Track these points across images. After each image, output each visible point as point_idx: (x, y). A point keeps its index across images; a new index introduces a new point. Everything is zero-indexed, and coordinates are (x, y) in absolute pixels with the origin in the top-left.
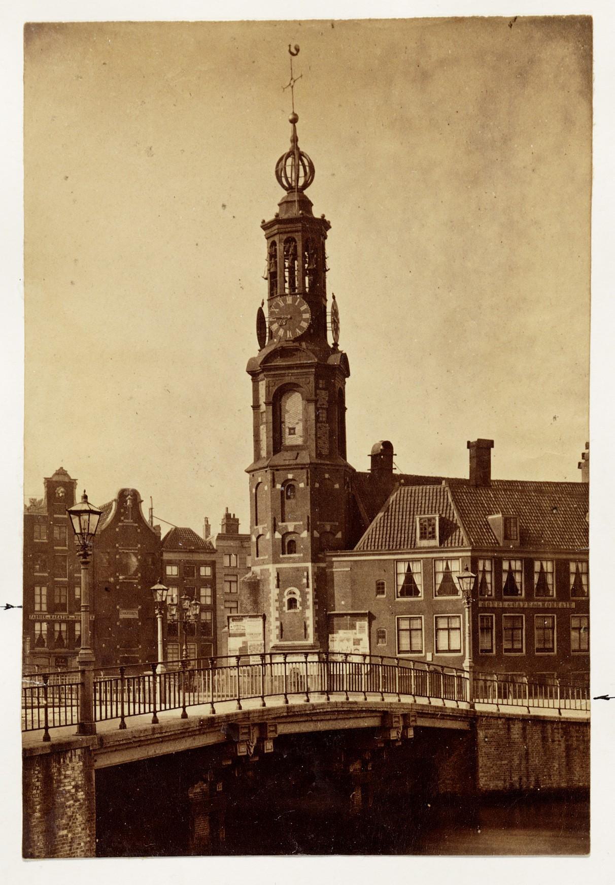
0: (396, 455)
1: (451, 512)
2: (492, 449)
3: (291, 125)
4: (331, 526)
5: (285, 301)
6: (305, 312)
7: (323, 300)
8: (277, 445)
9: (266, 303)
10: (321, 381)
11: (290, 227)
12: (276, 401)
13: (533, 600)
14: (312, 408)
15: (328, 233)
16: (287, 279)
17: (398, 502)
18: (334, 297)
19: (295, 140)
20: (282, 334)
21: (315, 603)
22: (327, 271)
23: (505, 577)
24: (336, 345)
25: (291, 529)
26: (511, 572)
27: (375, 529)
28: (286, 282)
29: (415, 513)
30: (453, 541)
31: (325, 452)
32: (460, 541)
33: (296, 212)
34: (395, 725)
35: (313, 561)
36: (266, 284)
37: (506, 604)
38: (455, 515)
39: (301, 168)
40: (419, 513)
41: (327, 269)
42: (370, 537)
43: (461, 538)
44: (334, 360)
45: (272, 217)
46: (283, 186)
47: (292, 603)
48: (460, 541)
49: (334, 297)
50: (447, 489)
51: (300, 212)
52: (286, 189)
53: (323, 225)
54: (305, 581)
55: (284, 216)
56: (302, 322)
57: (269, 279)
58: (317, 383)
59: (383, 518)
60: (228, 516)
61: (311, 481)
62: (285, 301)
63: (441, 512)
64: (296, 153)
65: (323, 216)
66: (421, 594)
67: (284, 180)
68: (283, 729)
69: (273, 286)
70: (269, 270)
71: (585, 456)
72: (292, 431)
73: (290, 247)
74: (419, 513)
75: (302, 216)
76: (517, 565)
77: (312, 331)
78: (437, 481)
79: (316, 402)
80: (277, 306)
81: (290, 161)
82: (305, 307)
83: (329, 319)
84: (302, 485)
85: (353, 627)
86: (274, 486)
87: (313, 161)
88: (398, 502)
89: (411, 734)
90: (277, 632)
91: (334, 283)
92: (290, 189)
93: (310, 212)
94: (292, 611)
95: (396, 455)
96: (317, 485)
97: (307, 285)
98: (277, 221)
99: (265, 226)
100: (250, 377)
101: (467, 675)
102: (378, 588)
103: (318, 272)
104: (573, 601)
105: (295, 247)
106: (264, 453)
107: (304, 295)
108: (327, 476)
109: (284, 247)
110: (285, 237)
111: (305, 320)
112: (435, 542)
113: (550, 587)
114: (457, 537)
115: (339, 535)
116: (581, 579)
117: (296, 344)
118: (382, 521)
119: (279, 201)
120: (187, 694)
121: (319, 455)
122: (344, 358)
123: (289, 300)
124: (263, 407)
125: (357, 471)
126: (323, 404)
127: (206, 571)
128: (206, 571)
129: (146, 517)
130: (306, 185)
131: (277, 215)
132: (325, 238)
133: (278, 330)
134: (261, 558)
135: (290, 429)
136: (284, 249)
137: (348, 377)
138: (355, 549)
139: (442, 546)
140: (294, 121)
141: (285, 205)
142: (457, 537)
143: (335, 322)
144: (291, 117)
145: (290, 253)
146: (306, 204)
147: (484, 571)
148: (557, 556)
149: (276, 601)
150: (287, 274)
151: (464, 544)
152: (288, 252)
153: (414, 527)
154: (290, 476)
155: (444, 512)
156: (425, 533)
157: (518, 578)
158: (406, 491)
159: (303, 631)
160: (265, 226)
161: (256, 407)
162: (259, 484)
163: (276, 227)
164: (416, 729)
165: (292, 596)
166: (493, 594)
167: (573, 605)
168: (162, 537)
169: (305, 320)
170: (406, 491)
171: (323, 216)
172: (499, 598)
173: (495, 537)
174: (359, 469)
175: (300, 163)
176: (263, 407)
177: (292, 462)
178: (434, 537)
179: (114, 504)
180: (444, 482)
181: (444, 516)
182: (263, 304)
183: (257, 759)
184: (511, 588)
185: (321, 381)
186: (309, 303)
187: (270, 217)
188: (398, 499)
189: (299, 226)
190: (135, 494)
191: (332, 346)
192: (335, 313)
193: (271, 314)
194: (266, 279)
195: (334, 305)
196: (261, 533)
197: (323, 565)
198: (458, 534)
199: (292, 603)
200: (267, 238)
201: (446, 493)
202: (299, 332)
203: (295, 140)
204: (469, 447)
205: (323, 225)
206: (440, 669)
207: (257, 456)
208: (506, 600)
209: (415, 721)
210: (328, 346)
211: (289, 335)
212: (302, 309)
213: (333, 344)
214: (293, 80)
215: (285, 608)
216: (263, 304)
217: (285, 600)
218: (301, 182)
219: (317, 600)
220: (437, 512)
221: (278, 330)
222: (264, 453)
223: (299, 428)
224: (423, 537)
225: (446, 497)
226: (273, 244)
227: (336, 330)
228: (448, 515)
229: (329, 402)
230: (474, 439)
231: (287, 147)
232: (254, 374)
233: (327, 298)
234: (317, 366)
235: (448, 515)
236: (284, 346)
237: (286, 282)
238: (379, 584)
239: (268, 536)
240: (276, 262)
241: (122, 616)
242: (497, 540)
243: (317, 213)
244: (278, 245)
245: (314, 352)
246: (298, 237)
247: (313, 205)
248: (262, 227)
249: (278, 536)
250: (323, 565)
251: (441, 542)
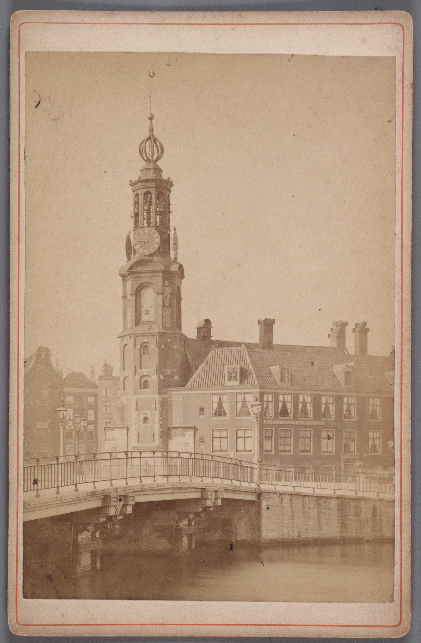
0: (213, 328)
1: (248, 364)
2: (274, 325)
3: (149, 121)
4: (171, 372)
5: (144, 231)
6: (156, 238)
7: (168, 230)
8: (138, 321)
9: (132, 232)
10: (166, 281)
11: (148, 184)
12: (137, 294)
13: (298, 420)
14: (160, 297)
15: (172, 189)
16: (145, 217)
17: (214, 358)
18: (175, 229)
19: (152, 130)
20: (141, 252)
21: (160, 420)
22: (171, 212)
23: (281, 405)
24: (176, 258)
25: (145, 374)
26: (284, 403)
27: (199, 375)
28: (144, 219)
29: (225, 365)
30: (248, 382)
31: (168, 325)
32: (253, 382)
33: (151, 175)
34: (209, 497)
35: (159, 394)
36: (132, 221)
37: (281, 422)
38: (250, 366)
39: (155, 148)
40: (227, 364)
41: (171, 211)
42: (196, 379)
43: (253, 380)
44: (174, 268)
45: (137, 179)
47: (145, 419)
48: (253, 382)
49: (175, 229)
50: (245, 349)
51: (155, 175)
52: (146, 161)
53: (168, 184)
54: (154, 406)
55: (143, 178)
56: (155, 244)
57: (134, 217)
58: (163, 282)
59: (204, 367)
60: (106, 365)
61: (159, 344)
62: (144, 231)
63: (241, 364)
64: (152, 139)
65: (169, 179)
66: (228, 415)
67: (144, 155)
68: (140, 499)
69: (136, 221)
70: (134, 212)
71: (333, 330)
72: (147, 312)
73: (147, 197)
74: (227, 364)
75: (155, 178)
76: (289, 398)
77: (161, 250)
78: (239, 344)
79: (163, 294)
80: (139, 234)
81: (148, 143)
82: (157, 235)
83: (172, 242)
84: (153, 346)
85: (184, 435)
86: (135, 346)
87: (163, 144)
88: (214, 358)
89: (219, 503)
90: (136, 437)
91: (174, 220)
92: (148, 160)
93: (161, 175)
94: (146, 425)
95: (213, 328)
96: (163, 346)
97: (158, 221)
98: (140, 181)
99: (132, 184)
100: (121, 278)
101: (255, 466)
102: (201, 411)
103: (165, 212)
104: (323, 421)
105: (151, 197)
106: (129, 326)
107: (156, 227)
108: (169, 340)
109: (144, 197)
110: (144, 191)
111: (156, 243)
112: (237, 383)
113: (309, 412)
114: (251, 380)
115: (176, 378)
116: (328, 408)
117: (151, 258)
118: (204, 369)
119: (141, 169)
120: (78, 476)
121: (164, 327)
122: (181, 267)
123: (147, 230)
124: (129, 297)
125: (189, 337)
126: (167, 296)
127: (91, 400)
128: (91, 400)
129: (54, 365)
130: (158, 158)
131: (140, 178)
132: (170, 192)
133: (139, 249)
134: (126, 391)
135: (146, 311)
136: (144, 198)
137: (183, 279)
138: (186, 386)
139: (242, 385)
140: (151, 118)
141: (145, 171)
142: (251, 380)
143: (176, 244)
144: (149, 116)
145: (148, 201)
146: (158, 170)
147: (268, 401)
148: (313, 393)
149: (136, 418)
150: (145, 214)
151: (255, 385)
152: (146, 200)
153: (224, 374)
154: (146, 340)
155: (243, 364)
156: (231, 377)
157: (289, 406)
158: (219, 351)
159: (152, 437)
160: (132, 184)
161: (125, 297)
162: (126, 345)
163: (139, 184)
164: (223, 500)
165: (146, 416)
166: (273, 415)
167: (323, 423)
168: (64, 378)
169: (156, 243)
170: (219, 351)
171: (169, 179)
172: (276, 418)
173: (275, 380)
174: (189, 336)
175: (155, 145)
176: (129, 297)
177: (147, 332)
178: (236, 380)
179: (34, 357)
180: (243, 345)
181: (242, 366)
183: (121, 517)
184: (284, 413)
185: (166, 281)
186: (158, 232)
187: (135, 178)
188: (214, 356)
189: (153, 184)
190: (47, 350)
191: (173, 259)
192: (176, 239)
193: (135, 239)
194: (132, 217)
195: (175, 234)
196: (126, 376)
197: (165, 396)
198: (251, 378)
199: (145, 419)
200: (133, 192)
201: (244, 352)
202: (153, 251)
203: (152, 130)
204: (259, 323)
205: (168, 184)
206: (238, 462)
207: (125, 328)
208: (281, 420)
209: (222, 495)
210: (171, 259)
211: (147, 252)
212: (155, 236)
213: (174, 258)
214: (151, 93)
215: (141, 423)
217: (141, 418)
218: (155, 156)
219: (161, 418)
220: (239, 364)
221: (139, 249)
222: (129, 326)
223: (152, 310)
224: (229, 379)
225: (244, 355)
226: (137, 195)
227: (176, 249)
228: (245, 366)
229: (171, 294)
230: (262, 319)
231: (147, 135)
232: (123, 276)
233: (171, 229)
234: (164, 272)
235: (245, 366)
236: (143, 259)
237: (144, 219)
238: (201, 409)
239: (131, 377)
240: (138, 206)
241: (38, 426)
242: (276, 382)
243: (165, 176)
244: (140, 195)
245: (161, 262)
246: (153, 191)
247: (162, 171)
248: (130, 184)
249: (137, 377)
250: (165, 396)
251: (241, 382)
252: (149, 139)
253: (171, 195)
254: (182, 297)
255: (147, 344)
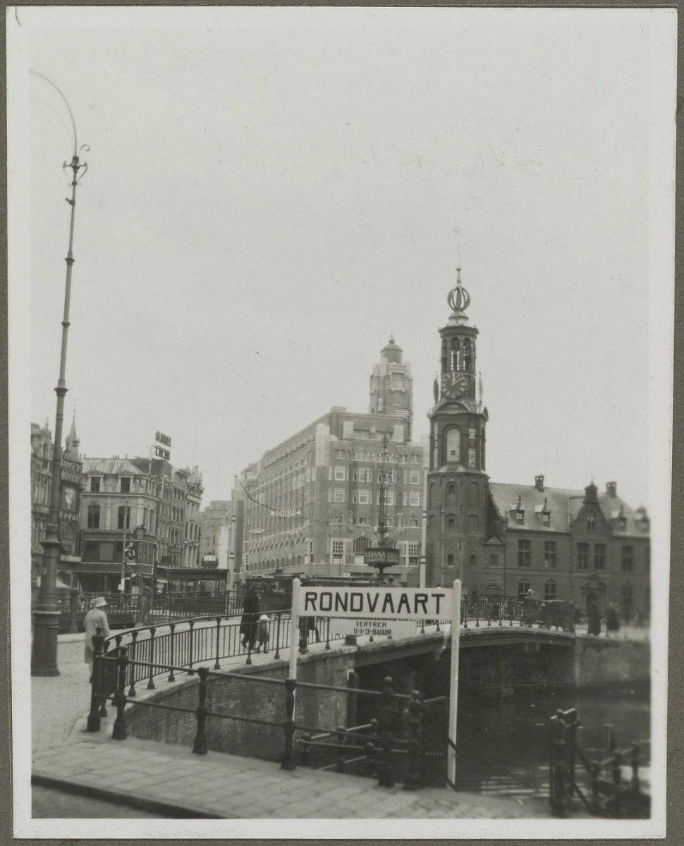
19: (459, 282)
24: (481, 402)
46: (451, 307)
52: (453, 309)
80: (446, 378)
97: (464, 366)
110: (453, 337)
130: (465, 307)
140: (459, 270)
143: (481, 388)
154: (452, 480)
169: (463, 387)
182: (437, 376)
193: (443, 382)
195: (480, 378)
203: (459, 282)
216: (437, 376)
218: (462, 306)
227: (481, 393)
231: (454, 285)
252: (458, 289)
253: (477, 342)
254: (486, 438)
255: (454, 484)
